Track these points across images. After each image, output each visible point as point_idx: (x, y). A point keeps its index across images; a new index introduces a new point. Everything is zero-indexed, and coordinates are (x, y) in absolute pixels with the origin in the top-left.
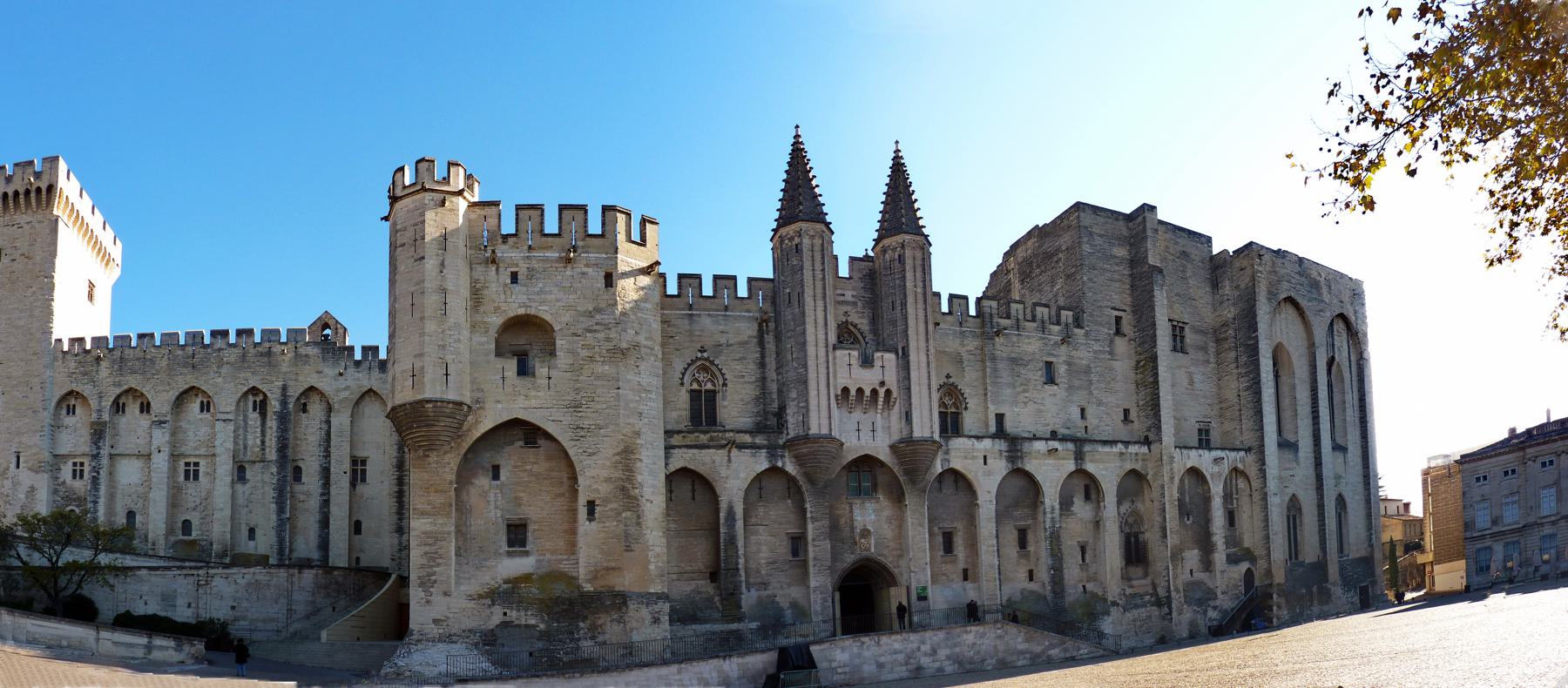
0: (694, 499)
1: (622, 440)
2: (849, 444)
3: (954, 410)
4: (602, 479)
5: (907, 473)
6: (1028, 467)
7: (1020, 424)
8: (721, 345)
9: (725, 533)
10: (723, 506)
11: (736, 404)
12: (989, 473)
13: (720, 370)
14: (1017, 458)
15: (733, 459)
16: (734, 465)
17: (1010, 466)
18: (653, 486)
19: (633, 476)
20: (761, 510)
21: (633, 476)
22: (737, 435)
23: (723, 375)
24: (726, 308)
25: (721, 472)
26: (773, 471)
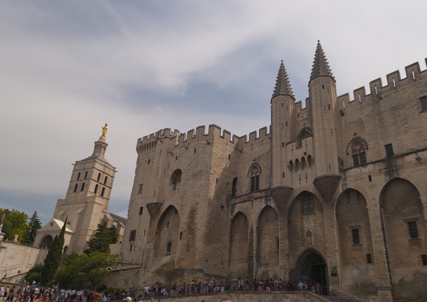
1: (191, 207)
2: (296, 188)
3: (362, 151)
4: (185, 223)
5: (323, 196)
6: (402, 176)
8: (260, 156)
9: (249, 239)
10: (250, 226)
13: (259, 166)
14: (393, 171)
15: (254, 205)
16: (254, 207)
17: (388, 178)
19: (194, 220)
20: (267, 226)
21: (194, 220)
22: (256, 194)
23: (260, 168)
24: (262, 141)
25: (250, 211)
26: (268, 207)
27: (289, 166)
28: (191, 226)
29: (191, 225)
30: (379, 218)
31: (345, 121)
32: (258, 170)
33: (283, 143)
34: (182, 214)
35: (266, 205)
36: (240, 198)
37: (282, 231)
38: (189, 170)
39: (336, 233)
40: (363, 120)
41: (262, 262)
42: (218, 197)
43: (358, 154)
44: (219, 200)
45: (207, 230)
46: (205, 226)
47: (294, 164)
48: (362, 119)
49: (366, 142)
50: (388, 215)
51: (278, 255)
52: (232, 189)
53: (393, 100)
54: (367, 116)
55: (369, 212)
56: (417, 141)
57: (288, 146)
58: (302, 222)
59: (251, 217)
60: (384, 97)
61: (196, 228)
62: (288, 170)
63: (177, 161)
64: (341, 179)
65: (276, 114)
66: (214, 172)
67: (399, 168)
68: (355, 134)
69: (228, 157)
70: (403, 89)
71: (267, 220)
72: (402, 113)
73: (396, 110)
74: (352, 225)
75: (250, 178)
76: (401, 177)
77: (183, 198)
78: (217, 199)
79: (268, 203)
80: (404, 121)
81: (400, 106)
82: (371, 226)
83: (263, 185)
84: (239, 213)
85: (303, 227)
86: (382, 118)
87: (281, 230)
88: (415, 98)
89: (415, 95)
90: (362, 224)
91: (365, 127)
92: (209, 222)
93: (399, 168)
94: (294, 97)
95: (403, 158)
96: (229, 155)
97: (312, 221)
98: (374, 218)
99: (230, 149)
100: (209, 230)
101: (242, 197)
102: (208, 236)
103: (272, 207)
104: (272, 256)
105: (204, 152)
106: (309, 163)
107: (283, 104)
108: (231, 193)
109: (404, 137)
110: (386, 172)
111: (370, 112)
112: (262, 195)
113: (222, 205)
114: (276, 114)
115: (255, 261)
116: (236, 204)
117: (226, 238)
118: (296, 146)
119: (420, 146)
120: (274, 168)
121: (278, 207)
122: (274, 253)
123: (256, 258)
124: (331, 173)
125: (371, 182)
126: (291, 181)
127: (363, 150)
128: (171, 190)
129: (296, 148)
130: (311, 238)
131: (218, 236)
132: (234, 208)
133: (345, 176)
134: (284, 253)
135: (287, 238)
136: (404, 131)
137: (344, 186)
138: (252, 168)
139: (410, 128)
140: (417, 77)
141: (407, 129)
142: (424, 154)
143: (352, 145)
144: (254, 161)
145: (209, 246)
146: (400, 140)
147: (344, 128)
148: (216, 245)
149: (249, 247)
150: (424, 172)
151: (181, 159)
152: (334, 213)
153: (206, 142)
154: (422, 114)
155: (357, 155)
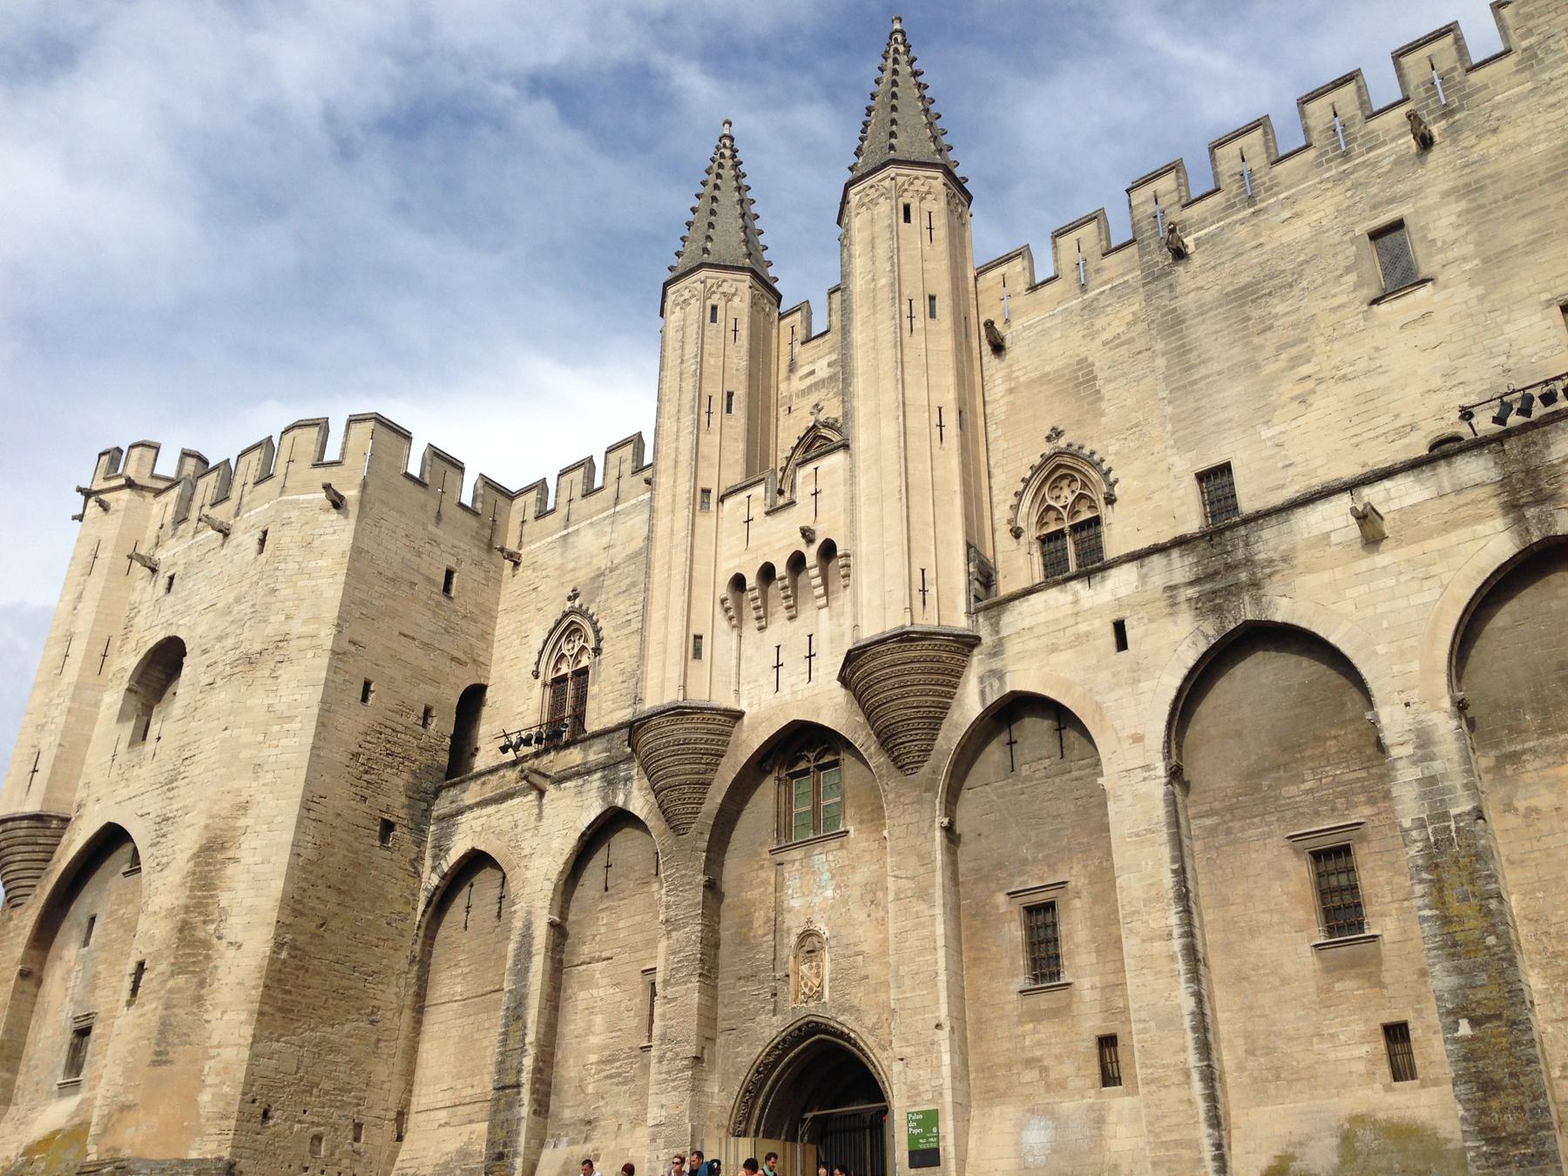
0: (499, 916)
1: (207, 826)
2: (755, 709)
3: (1086, 515)
4: (163, 913)
5: (886, 739)
6: (1283, 611)
7: (1291, 472)
8: (602, 574)
9: (510, 991)
10: (518, 924)
11: (613, 684)
12: (1136, 674)
14: (1233, 590)
15: (547, 811)
16: (545, 820)
18: (253, 910)
20: (604, 919)
23: (597, 632)
26: (614, 821)
27: (728, 604)
28: (194, 928)
29: (196, 919)
30: (1164, 835)
31: (1009, 377)
32: (586, 641)
33: (706, 492)
34: (159, 868)
35: (606, 807)
36: (484, 783)
37: (674, 934)
38: (220, 639)
39: (940, 929)
40: (1093, 365)
41: (567, 1114)
42: (366, 773)
43: (1067, 530)
44: (367, 793)
45: (279, 946)
46: (269, 924)
47: (754, 589)
48: (1090, 360)
49: (1105, 467)
50: (1208, 822)
51: (646, 1067)
52: (448, 741)
53: (1242, 254)
54: (1114, 343)
55: (1112, 807)
56: (1355, 440)
57: (728, 503)
58: (779, 887)
59: (529, 874)
60: (1197, 246)
61: (220, 938)
62: (722, 623)
63: (170, 598)
64: (976, 651)
65: (682, 355)
66: (353, 649)
67: (1267, 571)
68: (1056, 433)
69: (442, 580)
70: (1287, 198)
71: (606, 889)
72: (1285, 315)
73: (1252, 301)
74: (1024, 882)
75: (545, 685)
76: (1279, 617)
77: (174, 785)
78: (356, 782)
79: (614, 797)
80: (1294, 351)
81: (1276, 282)
82: (1118, 881)
83: (605, 710)
84: (476, 861)
85: (779, 908)
86: (1183, 346)
87: (669, 932)
88: (1347, 238)
89: (1348, 220)
90: (1075, 875)
91: (1101, 399)
92: (294, 906)
93: (1267, 571)
94: (776, 285)
95: (1287, 521)
96: (449, 574)
97: (826, 876)
98: (1138, 835)
99: (456, 542)
100: (294, 948)
101: (494, 779)
102: (279, 980)
103: (636, 813)
104: (619, 1075)
105: (307, 545)
106: (825, 583)
107: (714, 308)
108: (444, 759)
109: (1294, 424)
110: (1198, 599)
111: (1128, 324)
112: (592, 757)
113: (386, 816)
114: (682, 355)
115: (525, 1111)
116: (460, 812)
117: (393, 994)
118: (768, 501)
119: (1371, 463)
120: (656, 615)
121: (664, 811)
122: (629, 1057)
123: (534, 1091)
124: (927, 620)
125: (1123, 653)
126: (733, 680)
127: (1092, 507)
128: (123, 746)
129: (768, 513)
130: (818, 966)
131: (345, 983)
132: (449, 836)
133: (997, 632)
134: (677, 1054)
135: (695, 969)
136: (1292, 399)
137: (991, 685)
138: (557, 634)
139: (1320, 381)
140: (1355, 139)
141: (1310, 384)
142: (1393, 493)
143: (1039, 489)
144: (574, 596)
145: (281, 1036)
146: (1269, 444)
147: (1004, 409)
148: (330, 1030)
149: (503, 1034)
150: (1393, 582)
151: (190, 585)
152: (937, 825)
153: (323, 495)
154: (1384, 308)
155: (1059, 534)
